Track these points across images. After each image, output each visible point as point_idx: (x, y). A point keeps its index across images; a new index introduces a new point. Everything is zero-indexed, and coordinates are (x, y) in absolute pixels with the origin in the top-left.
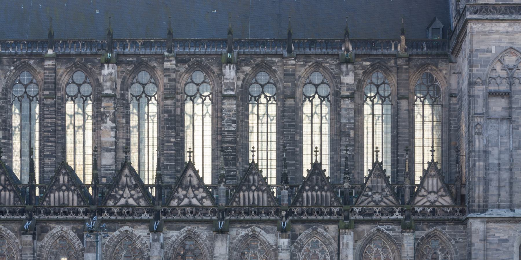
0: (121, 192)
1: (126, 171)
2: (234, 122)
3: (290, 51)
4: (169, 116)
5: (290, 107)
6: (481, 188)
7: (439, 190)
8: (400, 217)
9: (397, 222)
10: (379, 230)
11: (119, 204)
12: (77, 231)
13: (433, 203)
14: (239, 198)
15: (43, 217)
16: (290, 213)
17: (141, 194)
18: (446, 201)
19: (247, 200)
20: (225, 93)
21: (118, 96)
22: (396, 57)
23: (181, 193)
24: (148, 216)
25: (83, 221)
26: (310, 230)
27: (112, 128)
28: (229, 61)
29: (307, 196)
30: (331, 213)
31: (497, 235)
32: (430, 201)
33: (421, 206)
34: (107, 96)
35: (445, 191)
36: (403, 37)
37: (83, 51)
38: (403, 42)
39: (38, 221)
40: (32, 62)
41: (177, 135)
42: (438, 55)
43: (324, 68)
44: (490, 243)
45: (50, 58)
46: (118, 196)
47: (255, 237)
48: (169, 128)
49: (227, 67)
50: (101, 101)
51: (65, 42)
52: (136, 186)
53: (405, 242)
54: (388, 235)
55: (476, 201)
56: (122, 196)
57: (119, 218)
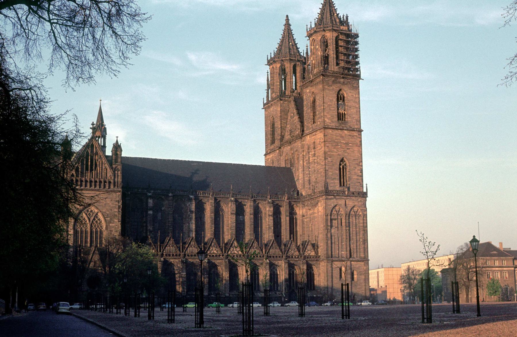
0: (212, 248)
40: (163, 197)
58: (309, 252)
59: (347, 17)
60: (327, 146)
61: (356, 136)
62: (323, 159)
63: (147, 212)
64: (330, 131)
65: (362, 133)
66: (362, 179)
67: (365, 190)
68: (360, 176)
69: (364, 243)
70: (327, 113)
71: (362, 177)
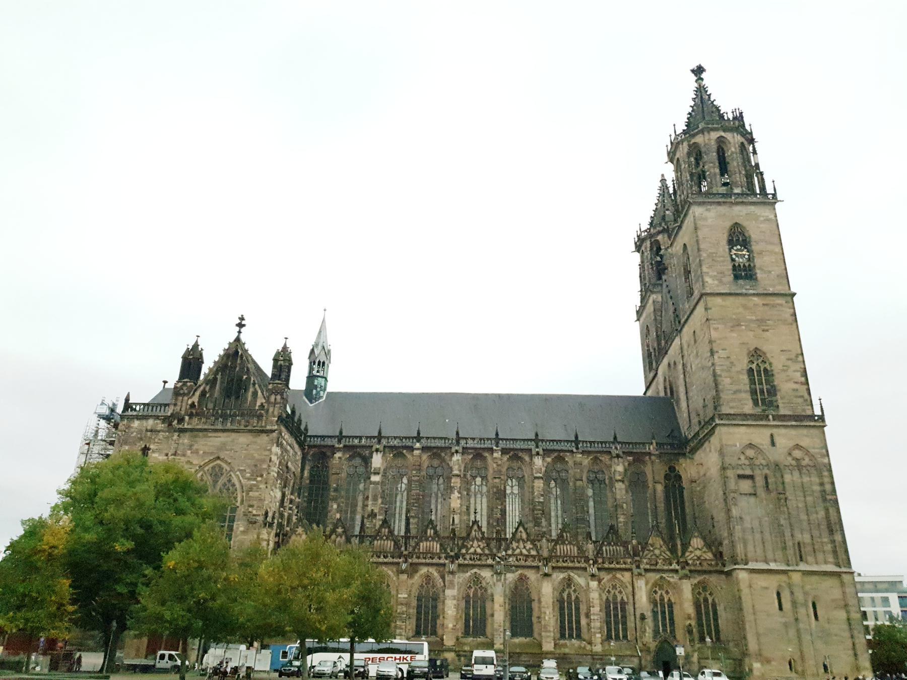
0: (471, 543)
1: (475, 527)
2: (542, 495)
3: (577, 448)
4: (498, 490)
5: (580, 487)
6: (742, 545)
7: (702, 548)
8: (677, 567)
9: (676, 571)
10: (661, 577)
11: (469, 552)
13: (699, 558)
14: (556, 549)
15: (415, 560)
16: (595, 562)
17: (485, 545)
18: (709, 556)
19: (562, 552)
20: (535, 475)
21: (462, 476)
22: (650, 454)
24: (492, 561)
25: (444, 565)
26: (611, 575)
27: (458, 497)
28: (538, 454)
29: (606, 550)
30: (625, 563)
31: (759, 583)
32: (696, 556)
33: (690, 559)
35: (707, 548)
36: (654, 441)
37: (439, 445)
38: (655, 444)
39: (411, 564)
40: (405, 451)
41: (502, 504)
42: (679, 454)
43: (601, 460)
44: (754, 590)
45: (418, 449)
46: (469, 546)
48: (497, 499)
49: (536, 457)
50: (451, 478)
51: (428, 438)
53: (684, 587)
54: (669, 581)
55: (739, 556)
56: (472, 546)
57: (471, 562)
58: (698, 553)
59: (742, 113)
61: (781, 305)
62: (709, 354)
63: (370, 478)
64: (719, 300)
65: (795, 298)
66: (808, 390)
67: (817, 412)
68: (802, 383)
69: (831, 532)
70: (710, 267)
71: (807, 384)
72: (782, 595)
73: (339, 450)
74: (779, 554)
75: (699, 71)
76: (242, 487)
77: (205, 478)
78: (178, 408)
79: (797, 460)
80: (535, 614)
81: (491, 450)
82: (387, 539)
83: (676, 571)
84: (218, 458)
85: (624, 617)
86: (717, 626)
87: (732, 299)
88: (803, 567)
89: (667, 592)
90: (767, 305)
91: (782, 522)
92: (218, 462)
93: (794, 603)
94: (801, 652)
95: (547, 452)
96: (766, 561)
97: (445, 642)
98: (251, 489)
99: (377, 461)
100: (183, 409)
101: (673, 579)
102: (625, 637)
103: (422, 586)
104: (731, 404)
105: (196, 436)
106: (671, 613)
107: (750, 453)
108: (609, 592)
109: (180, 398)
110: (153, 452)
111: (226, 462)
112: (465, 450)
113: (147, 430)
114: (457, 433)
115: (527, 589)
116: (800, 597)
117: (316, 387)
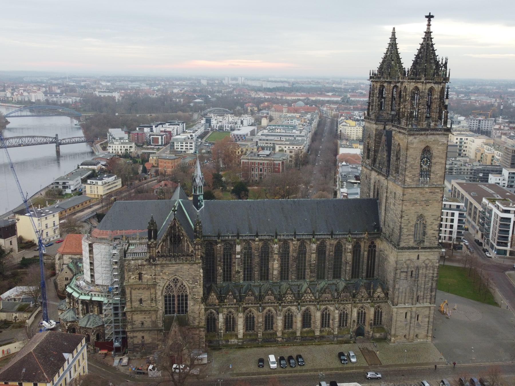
1: (289, 289)
2: (315, 260)
3: (332, 237)
9: (369, 303)
12: (274, 308)
15: (264, 305)
23: (305, 295)
25: (277, 306)
30: (350, 301)
34: (276, 254)
36: (367, 232)
47: (327, 307)
48: (294, 262)
52: (292, 294)
58: (379, 294)
60: (405, 205)
61: (438, 192)
64: (410, 190)
68: (437, 231)
70: (410, 172)
72: (407, 314)
73: (219, 243)
74: (410, 301)
75: (430, 17)
76: (189, 287)
77: (171, 283)
78: (152, 254)
79: (426, 265)
80: (312, 320)
81: (292, 240)
82: (251, 296)
83: (369, 303)
84: (175, 275)
85: (347, 318)
86: (381, 319)
87: (416, 189)
88: (417, 306)
89: (364, 309)
90: (431, 192)
91: (414, 289)
92: (176, 277)
93: (411, 317)
94: (409, 334)
95: (318, 239)
96: (405, 304)
97: (278, 335)
98: (193, 288)
99: (238, 248)
100: (154, 254)
101: (368, 305)
102: (346, 325)
103: (267, 313)
104: (405, 241)
105: (163, 266)
106: (365, 316)
107: (408, 262)
108: (342, 310)
109: (152, 249)
110: (144, 274)
111: (180, 277)
112: (280, 240)
113: (139, 265)
114: (276, 233)
115: (310, 311)
116: (414, 315)
117: (199, 200)
